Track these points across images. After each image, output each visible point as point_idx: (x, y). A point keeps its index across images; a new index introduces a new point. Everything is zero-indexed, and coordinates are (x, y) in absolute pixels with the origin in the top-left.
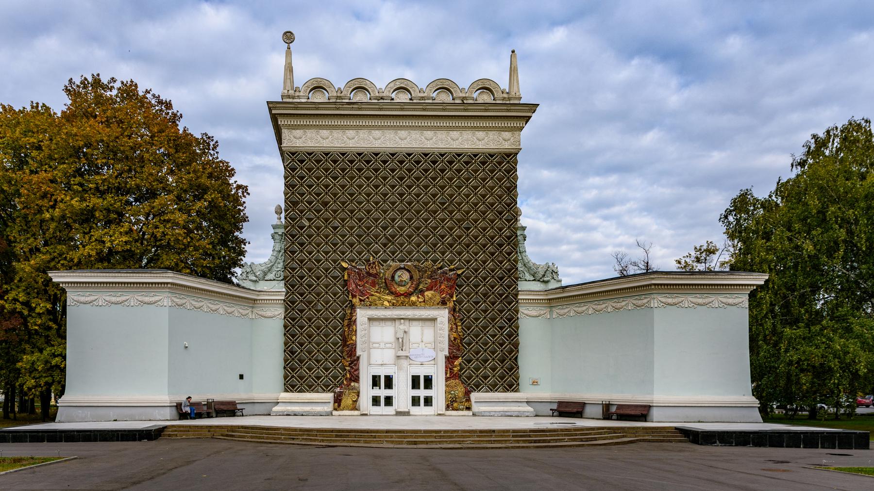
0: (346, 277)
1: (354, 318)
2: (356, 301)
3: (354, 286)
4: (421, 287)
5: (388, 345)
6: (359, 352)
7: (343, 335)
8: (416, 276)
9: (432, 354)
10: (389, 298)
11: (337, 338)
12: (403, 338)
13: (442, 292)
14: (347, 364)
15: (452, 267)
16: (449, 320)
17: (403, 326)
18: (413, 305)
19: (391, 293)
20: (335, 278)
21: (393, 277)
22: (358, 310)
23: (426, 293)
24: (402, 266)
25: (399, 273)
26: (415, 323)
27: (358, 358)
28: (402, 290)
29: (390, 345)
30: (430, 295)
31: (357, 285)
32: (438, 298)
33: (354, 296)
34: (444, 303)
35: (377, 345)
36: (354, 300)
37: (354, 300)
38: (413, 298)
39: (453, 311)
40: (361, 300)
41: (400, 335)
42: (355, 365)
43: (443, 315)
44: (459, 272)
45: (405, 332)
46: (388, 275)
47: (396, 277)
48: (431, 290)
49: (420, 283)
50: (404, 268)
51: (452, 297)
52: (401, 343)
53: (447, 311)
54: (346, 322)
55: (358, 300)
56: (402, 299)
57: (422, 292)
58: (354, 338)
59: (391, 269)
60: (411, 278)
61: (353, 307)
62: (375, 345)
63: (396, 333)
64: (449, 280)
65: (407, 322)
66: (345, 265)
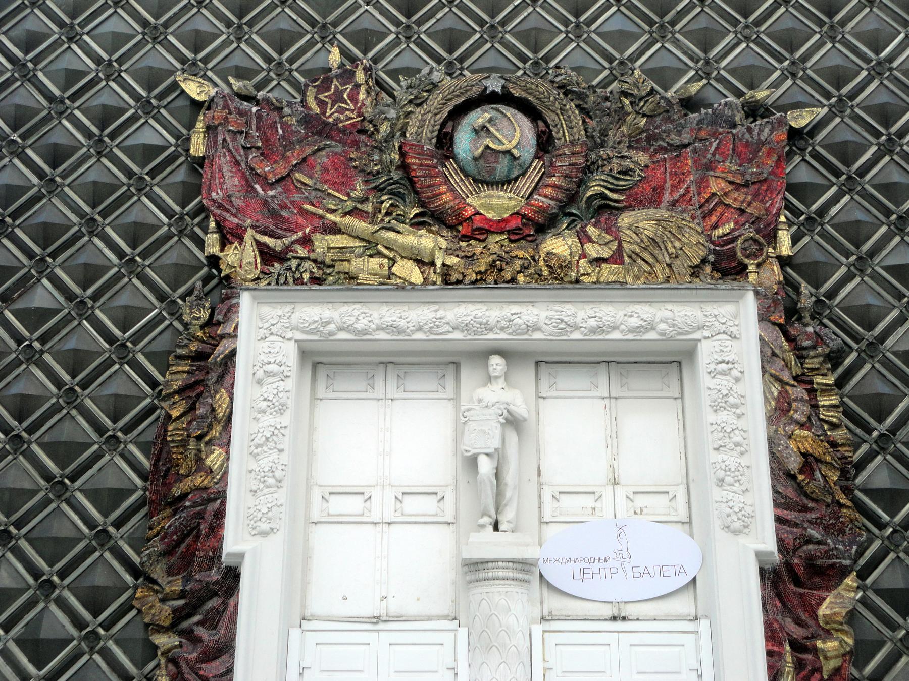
0: (198, 147)
1: (223, 348)
2: (241, 257)
3: (232, 181)
4: (594, 188)
5: (413, 505)
6: (235, 540)
7: (159, 449)
8: (569, 127)
9: (681, 552)
10: (425, 240)
11: (121, 471)
12: (499, 458)
13: (708, 211)
14: (164, 612)
15: (760, 95)
16: (768, 356)
17: (497, 392)
18: (559, 277)
19: (433, 217)
20: (148, 152)
21: (445, 141)
22: (245, 300)
23: (625, 220)
24: (495, 85)
25: (478, 117)
26: (570, 381)
27: (233, 576)
28: (495, 204)
29: (428, 505)
30: (648, 228)
31: (250, 178)
32: (693, 245)
33: (228, 236)
34: (726, 267)
35: (353, 505)
36: (230, 256)
37: (230, 256)
38: (559, 245)
39: (785, 314)
40: (267, 255)
41: (486, 435)
42: (211, 622)
43: (731, 330)
44: (801, 120)
45: (513, 422)
46: (422, 127)
47: (465, 144)
48: (654, 201)
49: (589, 169)
50: (504, 98)
51: (772, 238)
52: (489, 485)
53: (749, 305)
54: (178, 376)
55: (250, 253)
56: (500, 255)
57: (604, 209)
58: (214, 459)
59: (436, 99)
60: (545, 143)
61: (221, 287)
62: (339, 505)
63: (461, 425)
64: (748, 152)
65: (526, 376)
66: (193, 89)
